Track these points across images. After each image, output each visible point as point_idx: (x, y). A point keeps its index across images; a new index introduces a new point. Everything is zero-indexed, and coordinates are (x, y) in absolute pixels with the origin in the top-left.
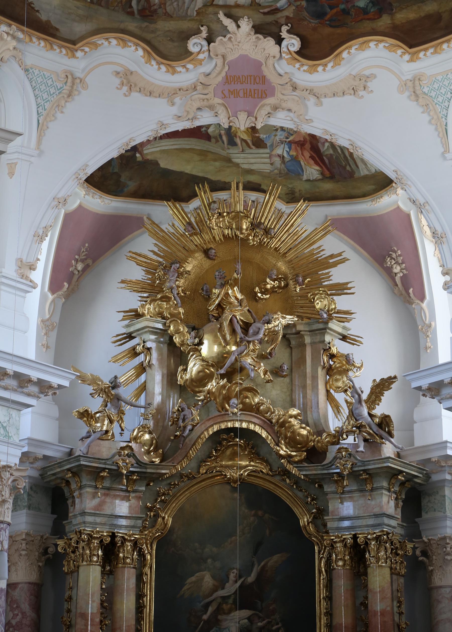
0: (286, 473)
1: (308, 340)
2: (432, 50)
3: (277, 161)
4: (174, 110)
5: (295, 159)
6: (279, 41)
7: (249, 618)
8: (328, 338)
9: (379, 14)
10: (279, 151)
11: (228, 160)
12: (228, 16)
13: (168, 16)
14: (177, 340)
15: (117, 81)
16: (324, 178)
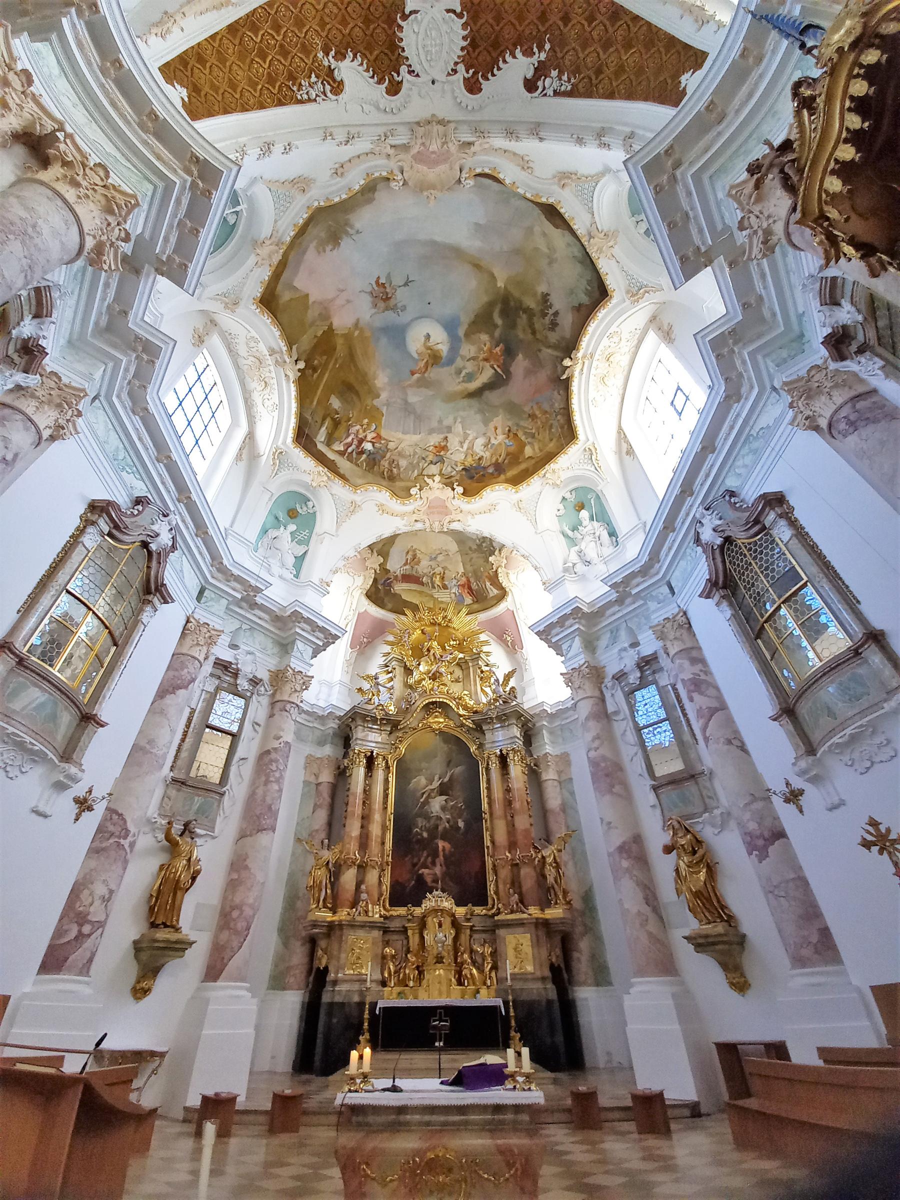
0: (463, 725)
1: (470, 664)
3: (453, 595)
4: (404, 522)
5: (461, 594)
6: (453, 489)
7: (446, 801)
8: (480, 663)
10: (453, 591)
11: (432, 596)
13: (402, 480)
14: (408, 663)
15: (377, 509)
16: (474, 602)
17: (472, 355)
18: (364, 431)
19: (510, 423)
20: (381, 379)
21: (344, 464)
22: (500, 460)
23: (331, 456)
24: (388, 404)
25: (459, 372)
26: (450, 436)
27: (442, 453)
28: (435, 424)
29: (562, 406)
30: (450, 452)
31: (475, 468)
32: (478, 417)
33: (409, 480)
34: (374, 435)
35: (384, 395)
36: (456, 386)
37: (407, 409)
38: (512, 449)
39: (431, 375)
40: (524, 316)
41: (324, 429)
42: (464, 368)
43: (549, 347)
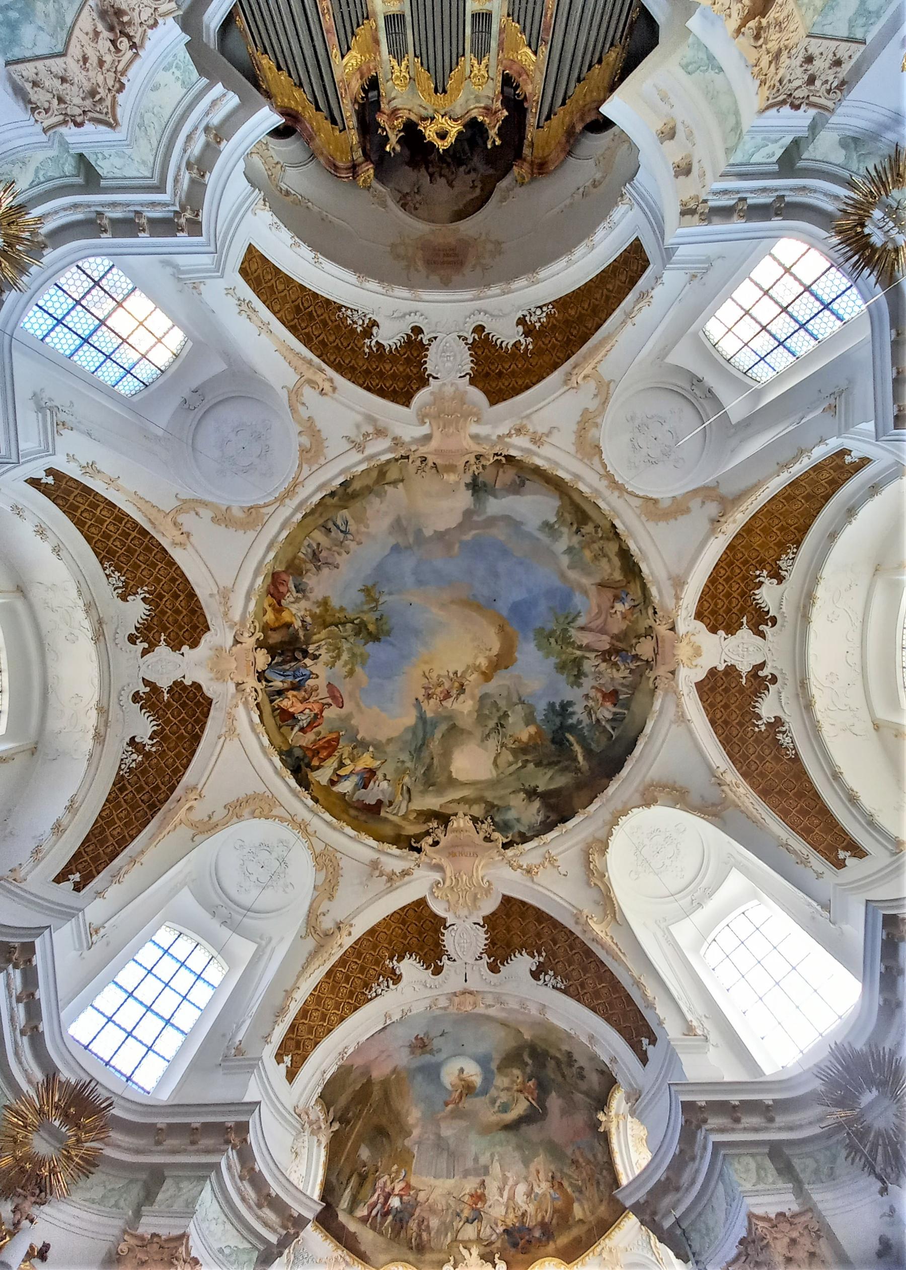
2: (580, 1263)
9: (548, 1240)
12: (465, 1248)
17: (506, 1085)
18: (392, 1182)
19: (553, 1167)
20: (414, 1115)
21: (367, 1237)
22: (546, 1220)
23: (353, 1226)
24: (419, 1143)
25: (493, 1102)
26: (488, 1180)
27: (479, 1206)
28: (470, 1164)
29: (605, 1160)
30: (488, 1203)
31: (519, 1230)
32: (517, 1154)
33: (440, 1251)
34: (402, 1185)
35: (416, 1132)
36: (491, 1116)
37: (440, 1145)
38: (559, 1204)
39: (466, 1105)
40: (553, 1062)
41: (348, 1190)
42: (498, 1097)
43: (581, 1092)
